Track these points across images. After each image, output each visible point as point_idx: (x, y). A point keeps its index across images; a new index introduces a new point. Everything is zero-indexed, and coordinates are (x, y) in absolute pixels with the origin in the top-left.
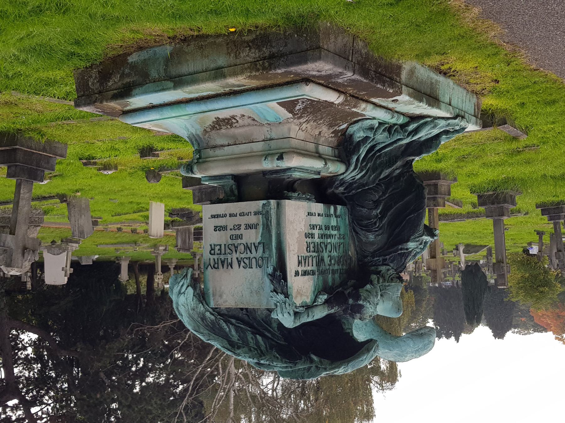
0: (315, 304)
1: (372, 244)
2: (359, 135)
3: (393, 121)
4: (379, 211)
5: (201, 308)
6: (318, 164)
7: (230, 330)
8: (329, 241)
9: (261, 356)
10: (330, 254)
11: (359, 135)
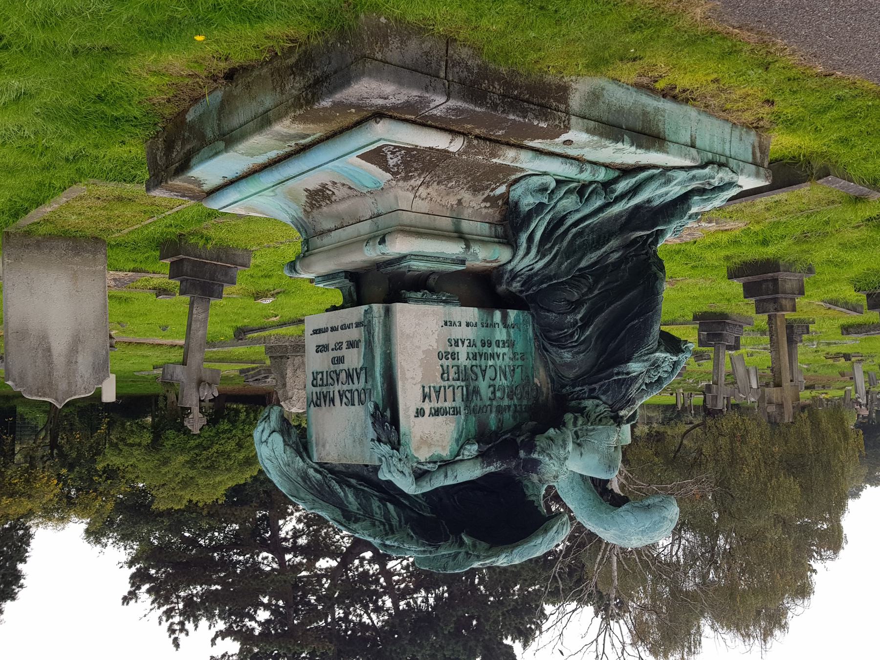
0: (460, 458)
1: (570, 366)
2: (528, 202)
3: (586, 176)
4: (579, 316)
5: (299, 463)
6: (454, 249)
7: (346, 495)
8: (490, 363)
9: (387, 534)
10: (492, 382)
11: (528, 202)
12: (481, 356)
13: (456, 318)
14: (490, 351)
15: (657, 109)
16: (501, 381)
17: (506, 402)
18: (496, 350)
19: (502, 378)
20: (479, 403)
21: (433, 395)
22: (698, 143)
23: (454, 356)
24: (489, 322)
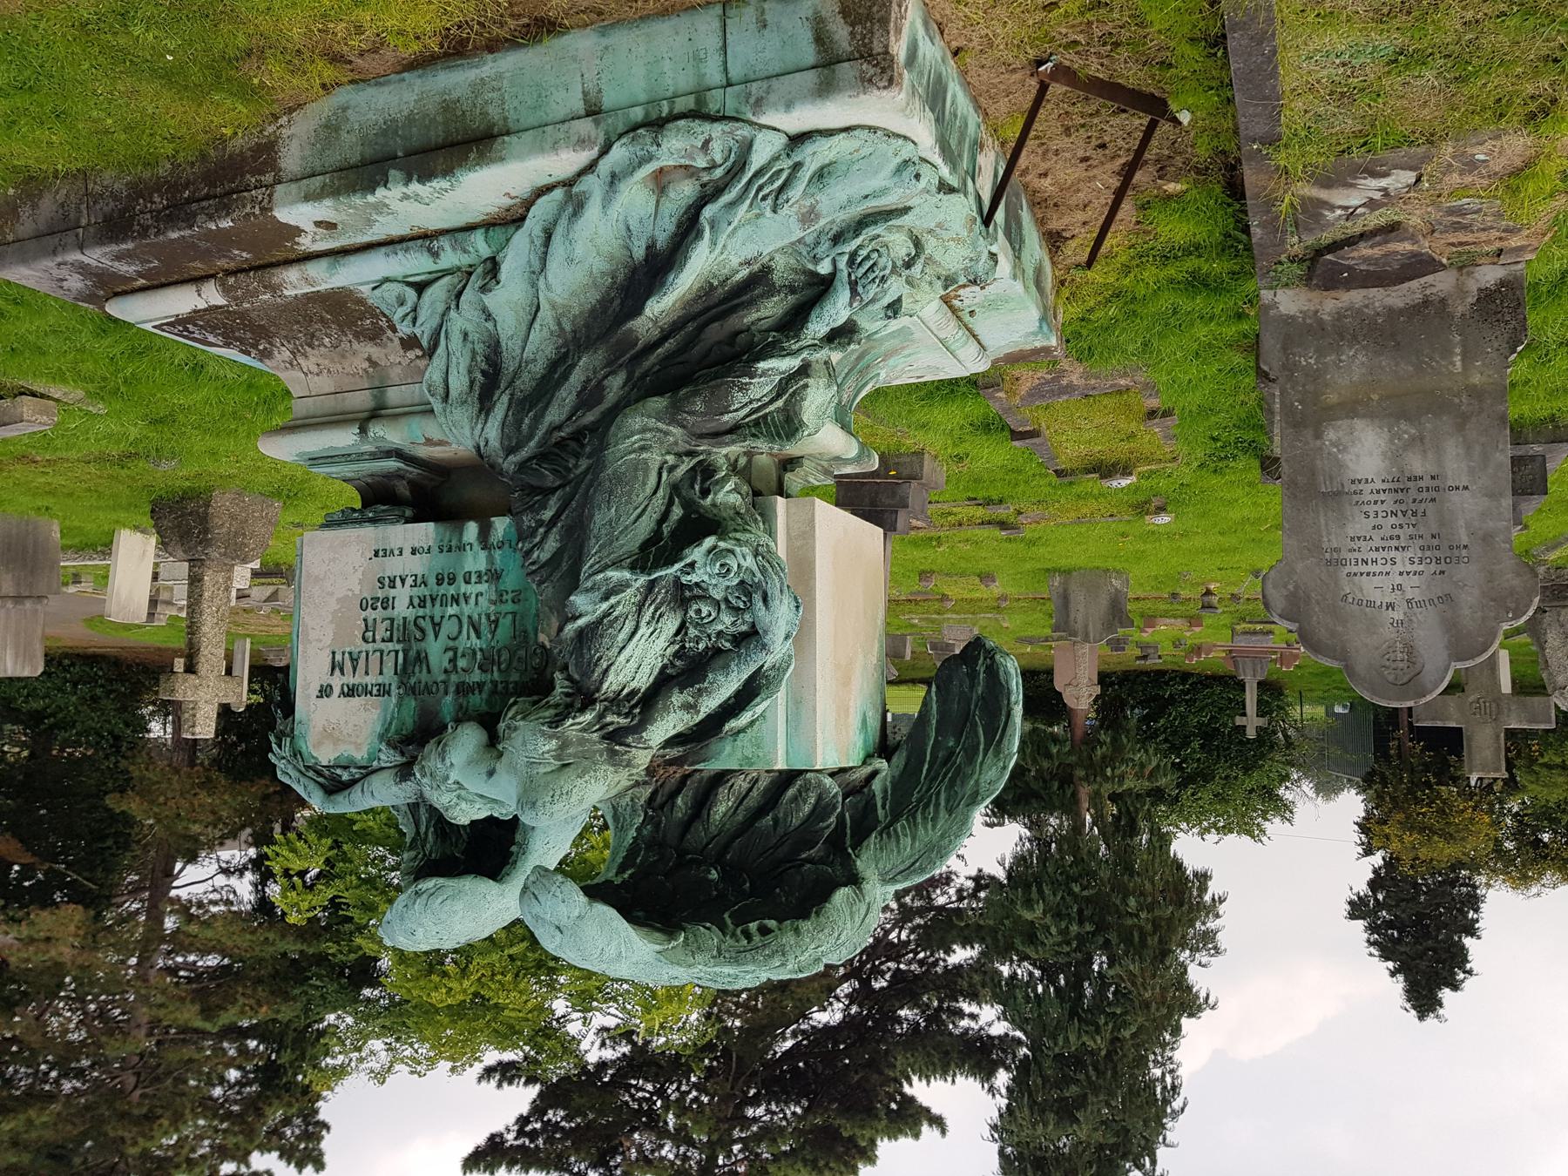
3: (450, 258)
4: (547, 515)
6: (344, 439)
8: (451, 610)
10: (451, 644)
12: (433, 600)
13: (394, 544)
14: (452, 590)
15: (478, 87)
17: (476, 676)
18: (464, 588)
19: (473, 634)
20: (424, 676)
21: (348, 664)
22: (608, 101)
23: (386, 603)
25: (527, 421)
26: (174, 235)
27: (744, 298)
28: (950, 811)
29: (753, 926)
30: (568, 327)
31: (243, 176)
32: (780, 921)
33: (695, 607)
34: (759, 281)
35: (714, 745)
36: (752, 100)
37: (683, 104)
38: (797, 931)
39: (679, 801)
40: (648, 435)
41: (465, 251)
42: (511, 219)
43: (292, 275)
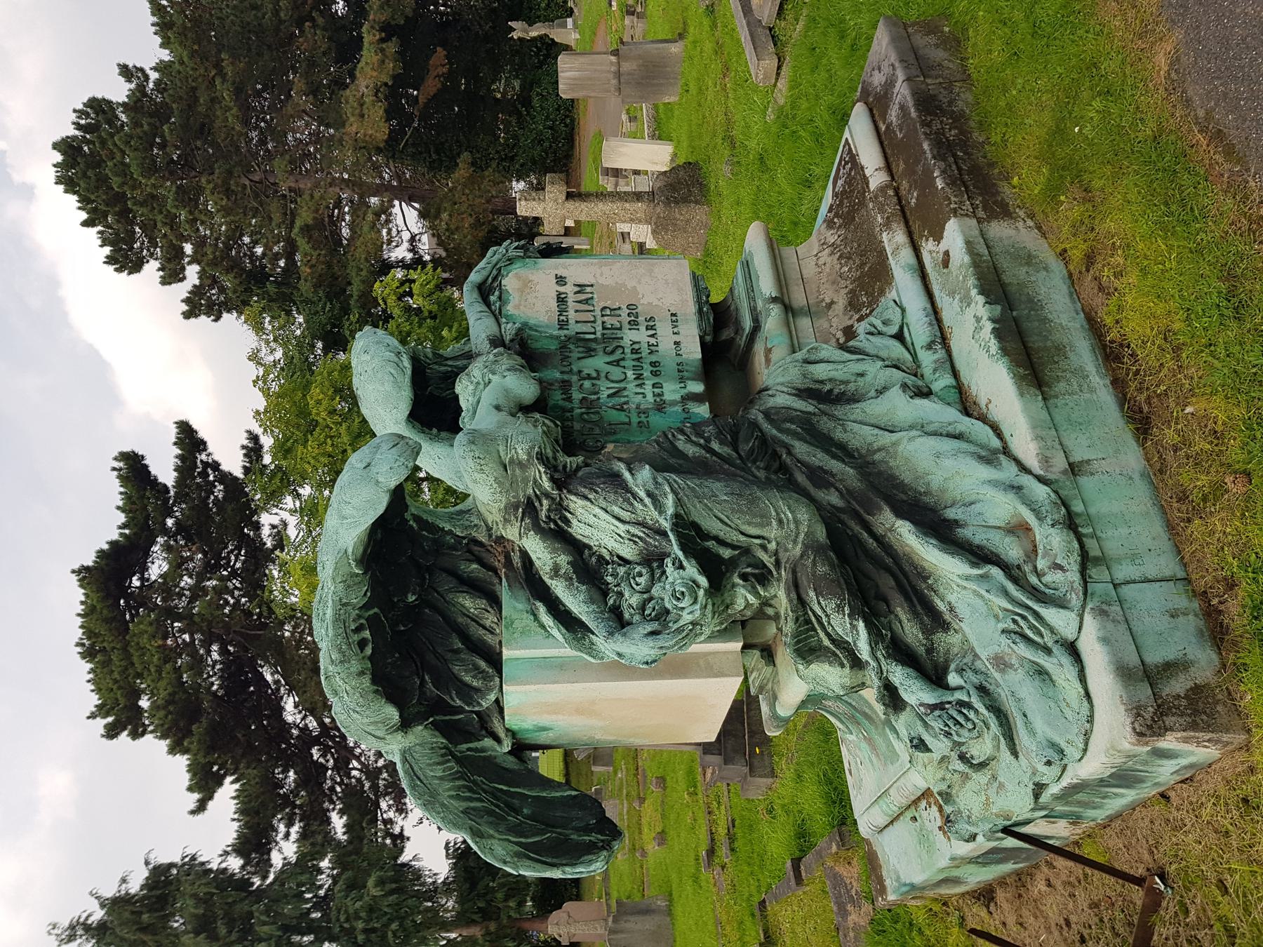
3: (927, 359)
4: (715, 445)
6: (766, 286)
8: (630, 374)
10: (603, 375)
12: (638, 360)
13: (682, 328)
14: (646, 374)
15: (1080, 373)
16: (605, 389)
17: (577, 396)
18: (649, 383)
20: (575, 355)
21: (583, 297)
22: (1084, 481)
23: (634, 324)
24: (685, 374)
25: (793, 427)
26: (926, 146)
27: (919, 608)
28: (465, 812)
29: (367, 634)
30: (877, 457)
31: (981, 194)
32: (371, 658)
33: (644, 571)
34: (935, 621)
35: (523, 594)
36: (1105, 607)
37: (1091, 544)
38: (361, 673)
39: (475, 566)
40: (792, 526)
41: (935, 370)
42: (966, 405)
43: (900, 237)
